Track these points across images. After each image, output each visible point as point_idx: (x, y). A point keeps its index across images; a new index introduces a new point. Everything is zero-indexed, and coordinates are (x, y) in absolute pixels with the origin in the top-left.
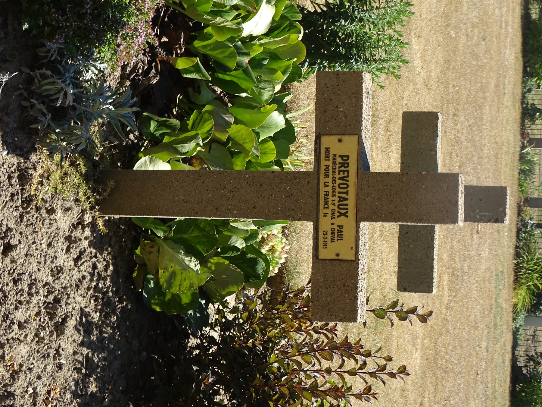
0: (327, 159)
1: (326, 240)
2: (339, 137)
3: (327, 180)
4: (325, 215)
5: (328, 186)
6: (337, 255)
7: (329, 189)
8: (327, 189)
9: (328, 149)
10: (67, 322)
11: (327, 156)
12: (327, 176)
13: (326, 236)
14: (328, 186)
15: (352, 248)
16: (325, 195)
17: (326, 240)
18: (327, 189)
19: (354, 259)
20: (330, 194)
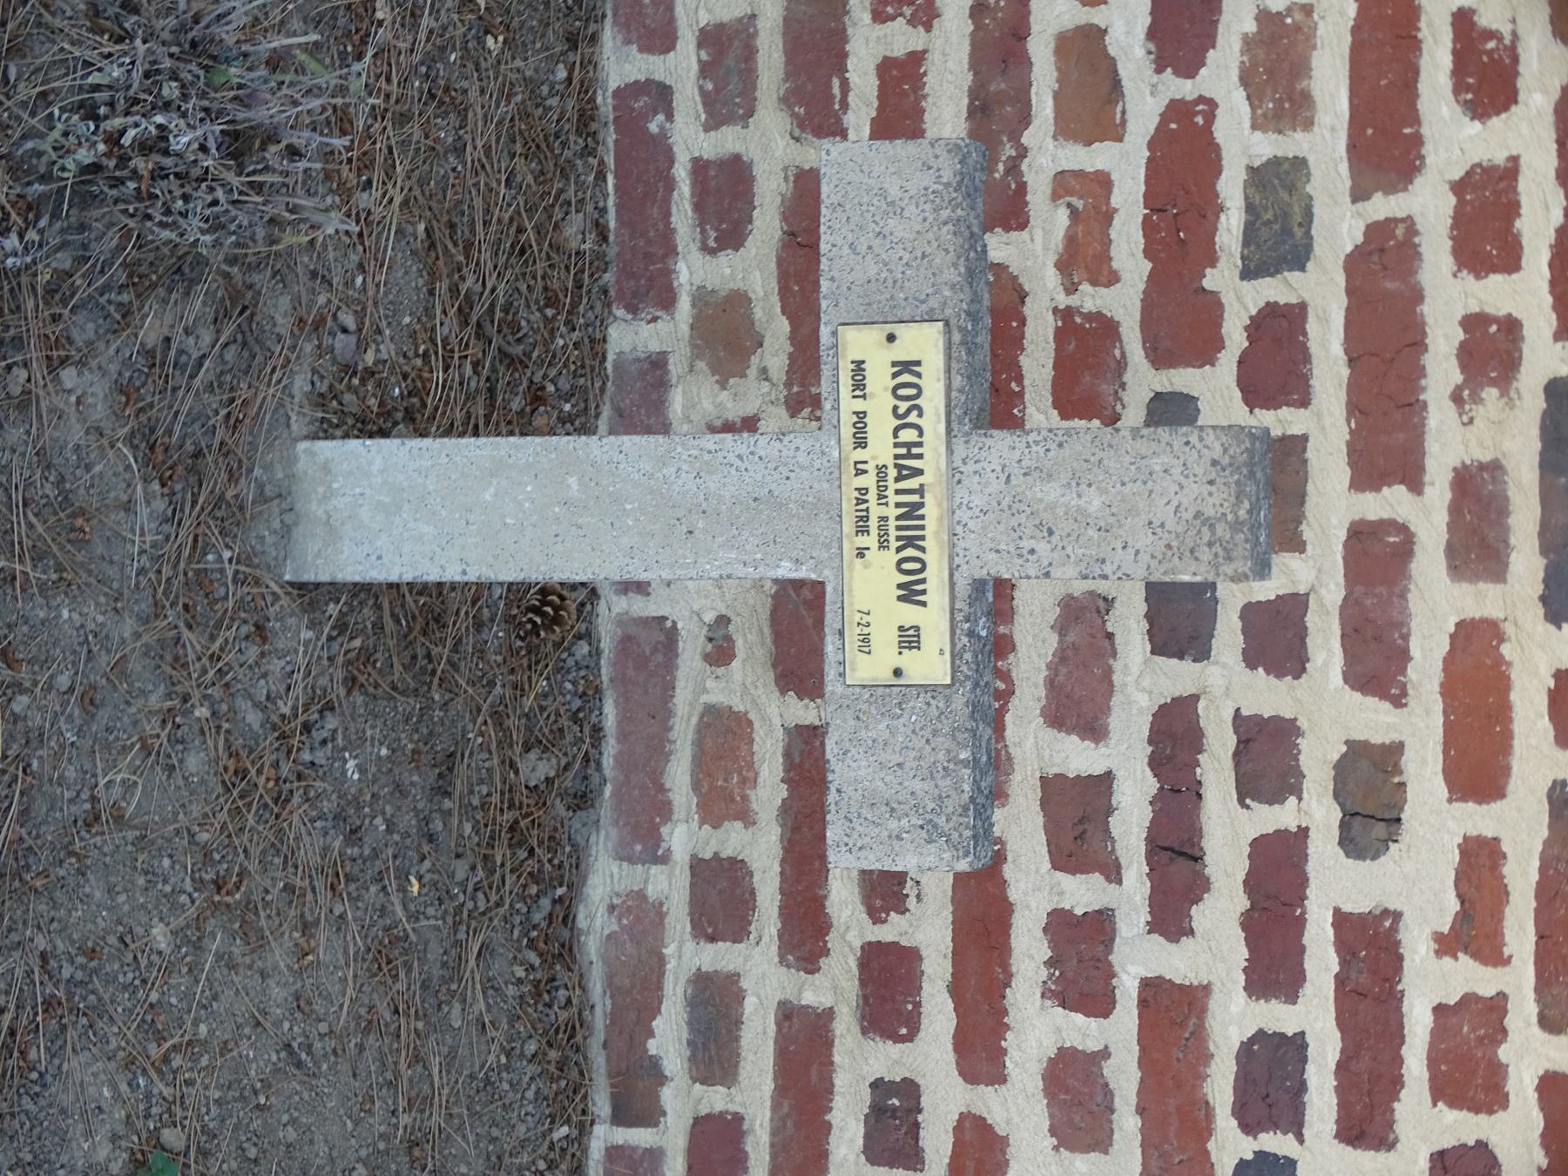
0: (858, 393)
1: (866, 630)
2: (889, 328)
3: (860, 454)
4: (861, 555)
5: (865, 472)
6: (897, 672)
7: (869, 480)
8: (861, 481)
9: (859, 365)
10: (651, 1034)
11: (859, 385)
12: (861, 443)
13: (866, 619)
14: (865, 472)
15: (942, 652)
16: (860, 501)
17: (866, 630)
18: (861, 481)
19: (948, 681)
20: (872, 496)
